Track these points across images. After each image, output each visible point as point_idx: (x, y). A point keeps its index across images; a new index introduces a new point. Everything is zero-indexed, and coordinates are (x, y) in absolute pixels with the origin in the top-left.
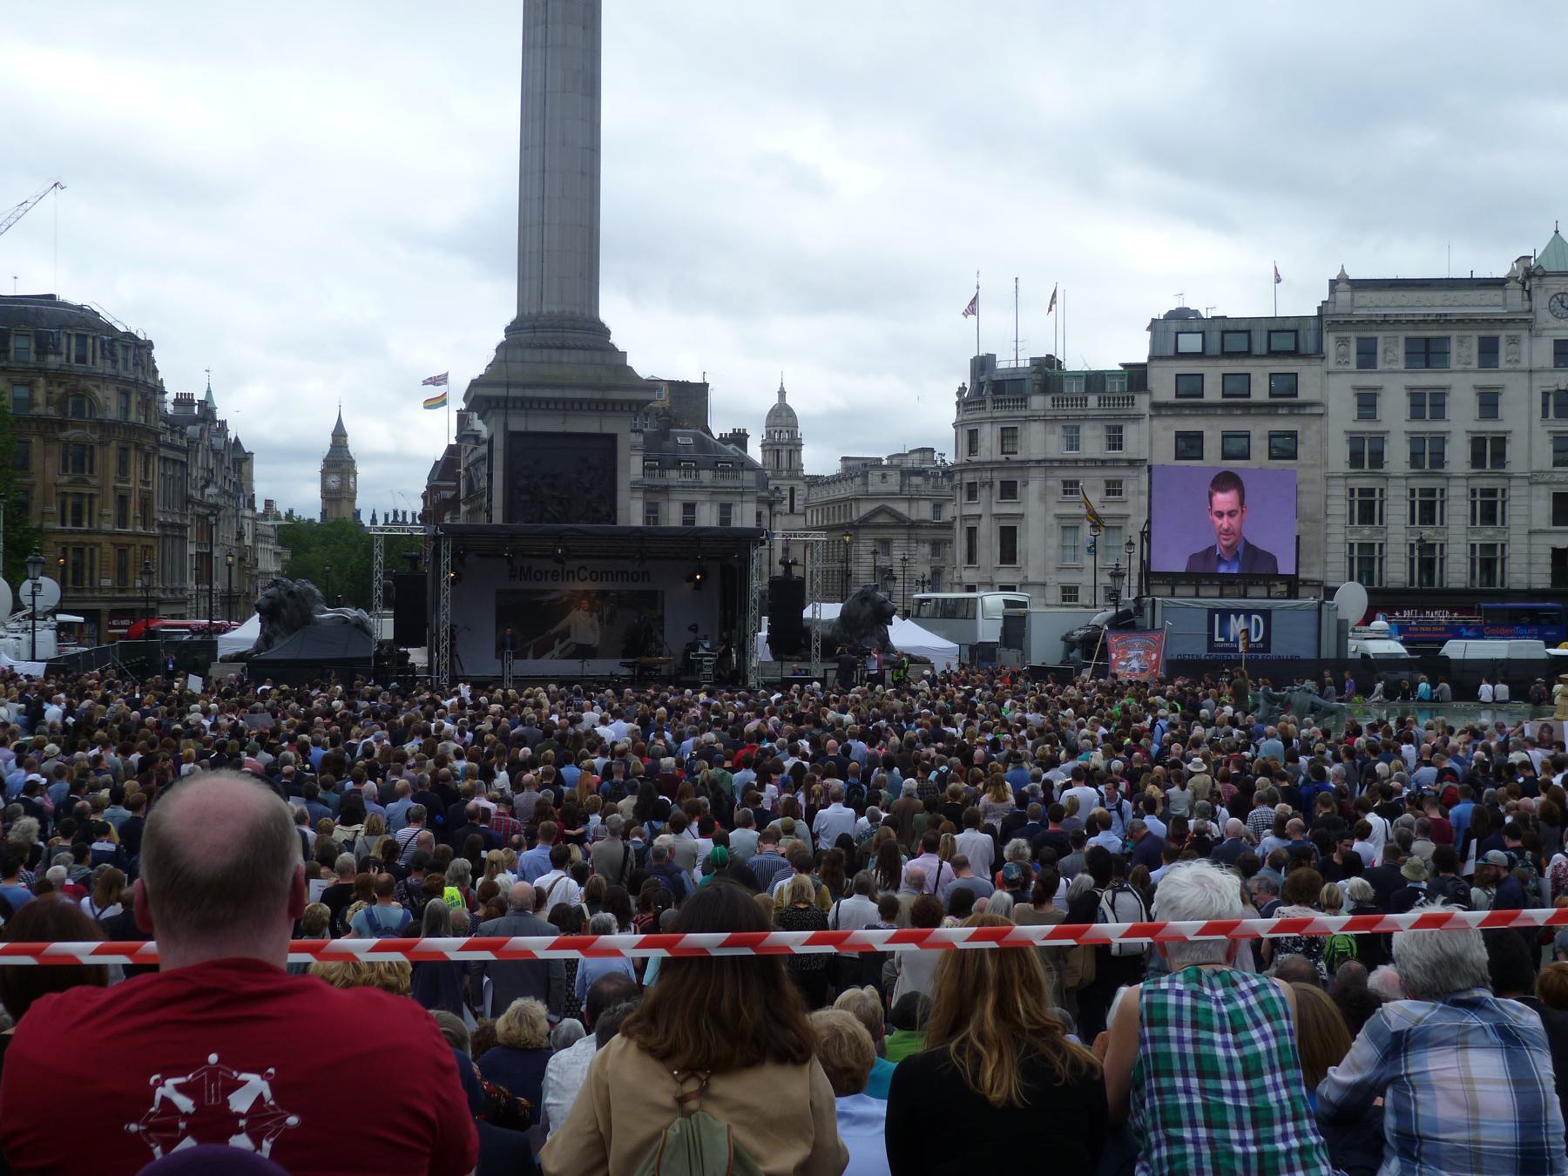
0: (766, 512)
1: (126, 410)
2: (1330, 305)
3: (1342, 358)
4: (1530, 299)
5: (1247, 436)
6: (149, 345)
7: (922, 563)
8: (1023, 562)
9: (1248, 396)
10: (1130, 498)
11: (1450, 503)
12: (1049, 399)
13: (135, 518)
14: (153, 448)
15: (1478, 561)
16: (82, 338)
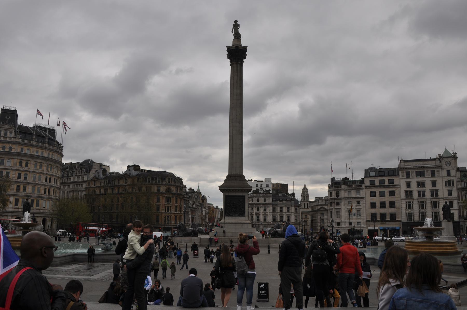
0: (298, 208)
1: (177, 191)
2: (400, 166)
3: (403, 176)
4: (441, 162)
5: (384, 192)
9: (384, 184)
10: (362, 205)
11: (427, 204)
12: (345, 186)
13: (178, 210)
14: (182, 198)
15: (434, 216)
16: (169, 179)
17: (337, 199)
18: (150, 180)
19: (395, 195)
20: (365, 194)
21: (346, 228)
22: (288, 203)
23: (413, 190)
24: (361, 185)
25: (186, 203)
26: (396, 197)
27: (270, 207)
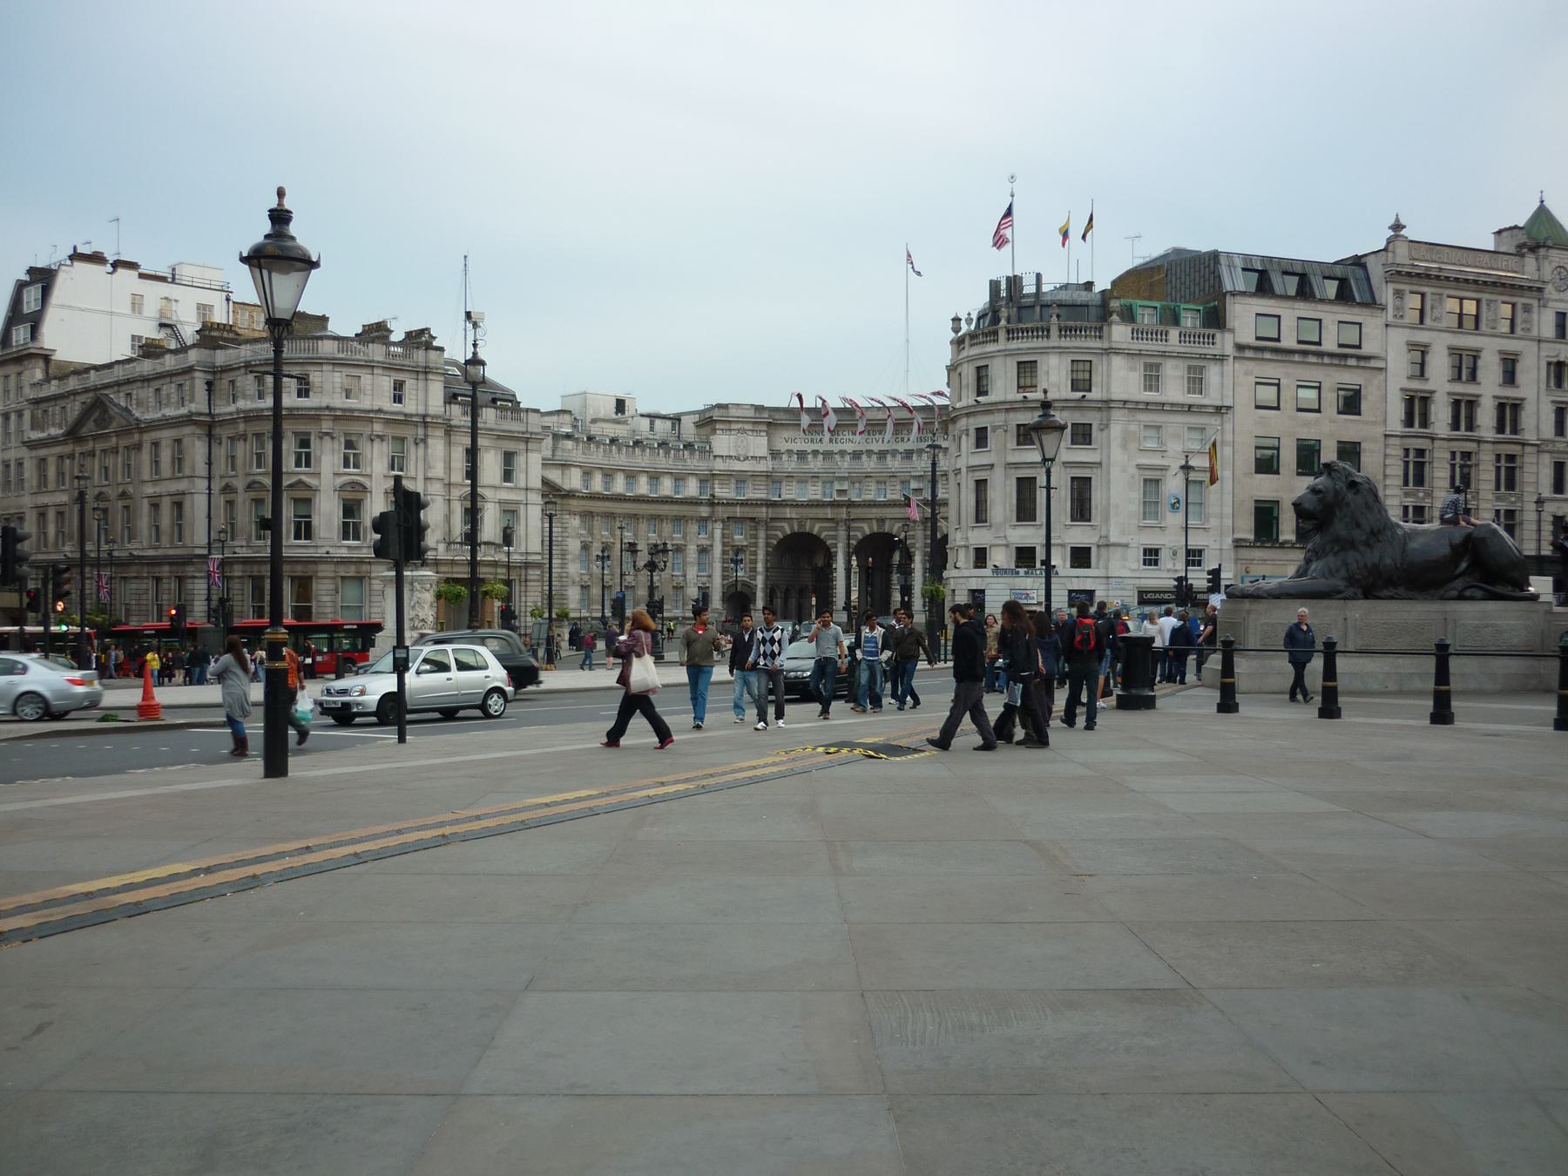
4: (1539, 270)
7: (573, 537)
17: (1085, 404)
19: (1364, 406)
21: (1133, 581)
22: (513, 428)
23: (1433, 392)
24: (1213, 339)
26: (1367, 423)
27: (430, 441)
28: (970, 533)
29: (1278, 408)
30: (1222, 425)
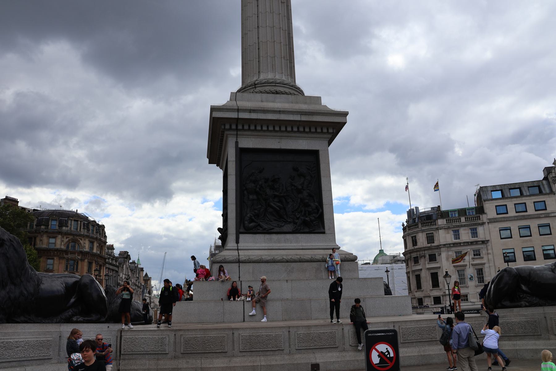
5: (528, 227)
6: (103, 227)
8: (442, 286)
10: (485, 258)
12: (445, 220)
18: (35, 223)
20: (490, 233)
24: (479, 218)
25: (112, 275)
28: (415, 294)
29: (511, 237)
30: (487, 247)
